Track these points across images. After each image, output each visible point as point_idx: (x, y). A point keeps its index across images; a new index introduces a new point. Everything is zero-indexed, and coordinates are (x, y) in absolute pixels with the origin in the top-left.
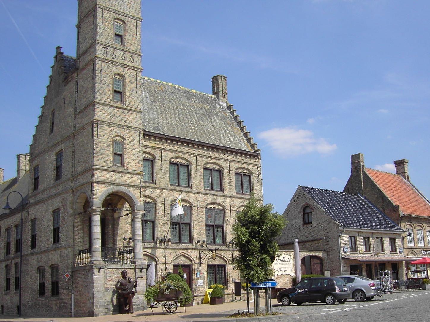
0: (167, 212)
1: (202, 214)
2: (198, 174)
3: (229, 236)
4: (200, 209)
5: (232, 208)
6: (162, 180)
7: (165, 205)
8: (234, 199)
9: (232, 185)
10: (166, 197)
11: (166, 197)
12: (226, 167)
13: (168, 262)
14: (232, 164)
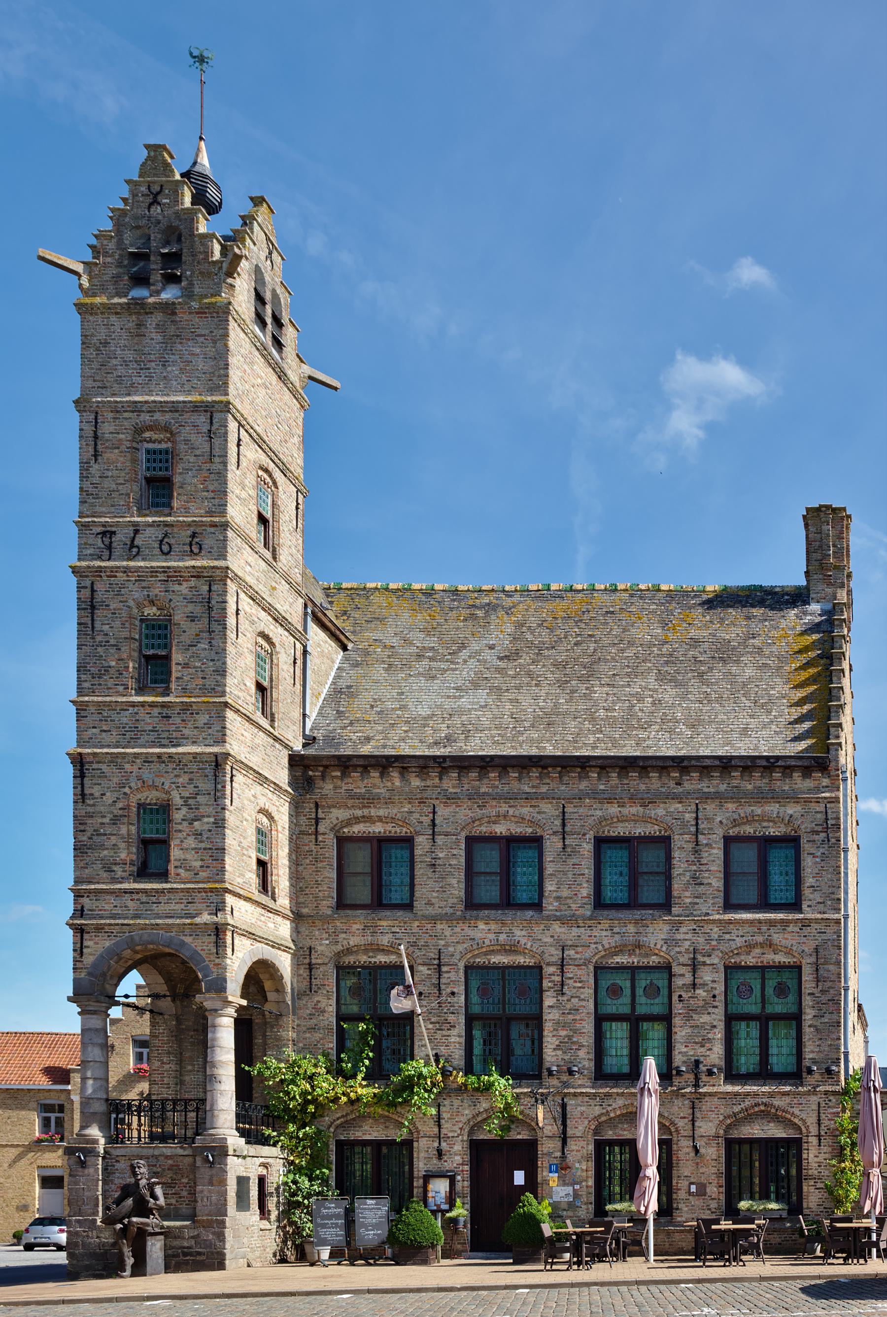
0: (449, 990)
1: (580, 985)
2: (571, 861)
3: (685, 1050)
4: (571, 971)
5: (700, 958)
6: (435, 894)
7: (444, 969)
8: (711, 926)
9: (705, 881)
10: (446, 945)
11: (446, 945)
12: (684, 824)
13: (450, 1135)
14: (710, 808)
